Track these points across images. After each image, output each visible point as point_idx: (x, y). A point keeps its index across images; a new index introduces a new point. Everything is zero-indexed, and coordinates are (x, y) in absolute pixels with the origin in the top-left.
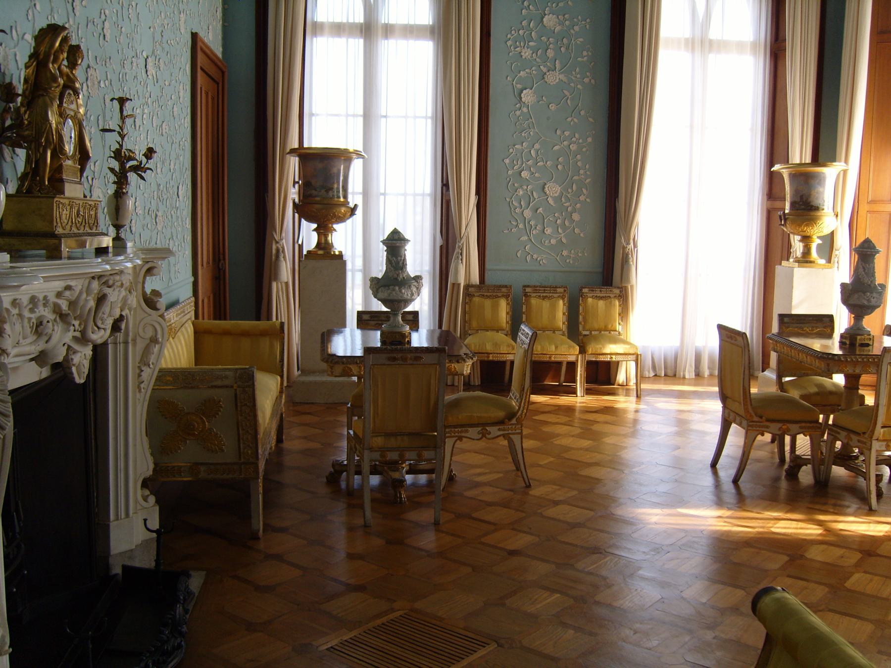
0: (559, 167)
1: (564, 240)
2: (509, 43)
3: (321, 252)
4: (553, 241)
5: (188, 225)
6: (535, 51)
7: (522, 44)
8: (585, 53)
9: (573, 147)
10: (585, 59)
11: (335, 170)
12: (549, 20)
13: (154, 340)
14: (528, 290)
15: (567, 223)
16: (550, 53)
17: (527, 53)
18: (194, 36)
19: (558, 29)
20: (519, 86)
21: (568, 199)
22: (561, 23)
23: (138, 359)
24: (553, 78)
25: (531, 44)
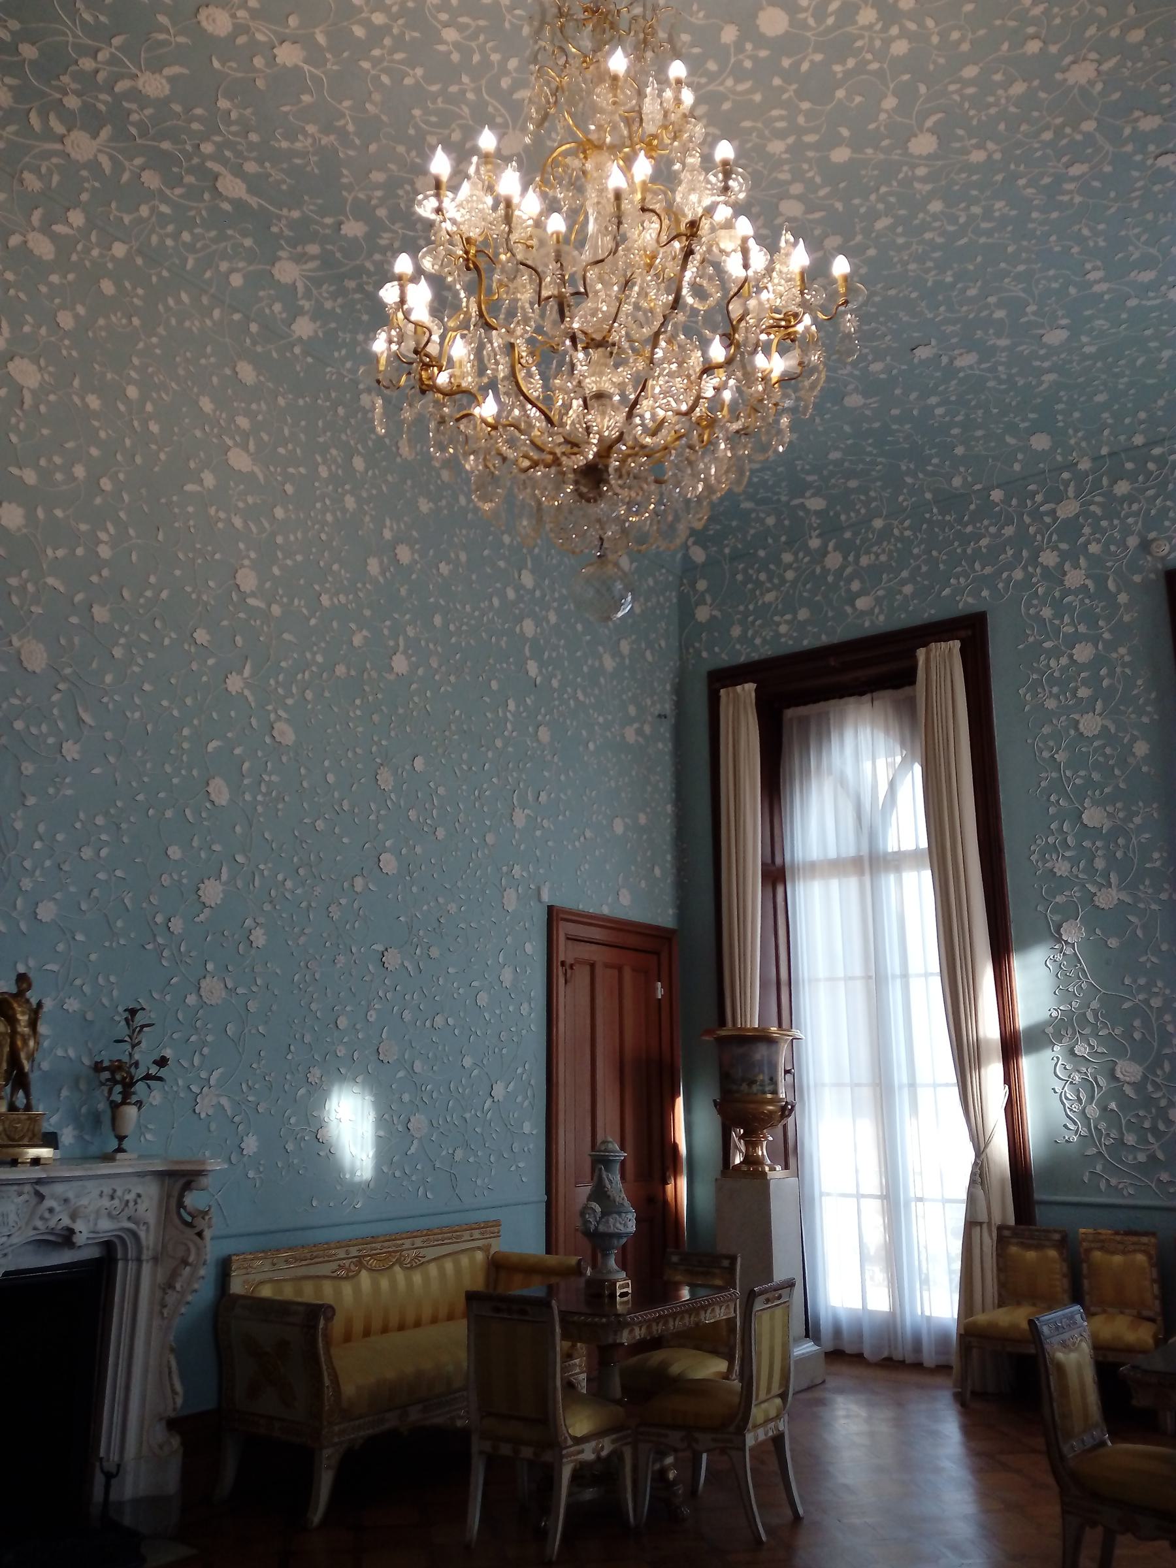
0: (1137, 1036)
1: (1160, 1156)
2: (1034, 858)
3: (745, 1168)
4: (1142, 1157)
5: (532, 1128)
6: (1074, 861)
7: (1054, 857)
8: (1156, 855)
9: (1156, 1002)
10: (1158, 864)
11: (758, 1057)
12: (1093, 816)
13: (185, 1262)
14: (1006, 1233)
15: (1162, 1127)
16: (1100, 864)
17: (1062, 868)
18: (550, 909)
19: (1107, 825)
20: (1057, 918)
21: (1157, 1086)
22: (1110, 816)
23: (160, 1278)
24: (1107, 898)
25: (1067, 854)
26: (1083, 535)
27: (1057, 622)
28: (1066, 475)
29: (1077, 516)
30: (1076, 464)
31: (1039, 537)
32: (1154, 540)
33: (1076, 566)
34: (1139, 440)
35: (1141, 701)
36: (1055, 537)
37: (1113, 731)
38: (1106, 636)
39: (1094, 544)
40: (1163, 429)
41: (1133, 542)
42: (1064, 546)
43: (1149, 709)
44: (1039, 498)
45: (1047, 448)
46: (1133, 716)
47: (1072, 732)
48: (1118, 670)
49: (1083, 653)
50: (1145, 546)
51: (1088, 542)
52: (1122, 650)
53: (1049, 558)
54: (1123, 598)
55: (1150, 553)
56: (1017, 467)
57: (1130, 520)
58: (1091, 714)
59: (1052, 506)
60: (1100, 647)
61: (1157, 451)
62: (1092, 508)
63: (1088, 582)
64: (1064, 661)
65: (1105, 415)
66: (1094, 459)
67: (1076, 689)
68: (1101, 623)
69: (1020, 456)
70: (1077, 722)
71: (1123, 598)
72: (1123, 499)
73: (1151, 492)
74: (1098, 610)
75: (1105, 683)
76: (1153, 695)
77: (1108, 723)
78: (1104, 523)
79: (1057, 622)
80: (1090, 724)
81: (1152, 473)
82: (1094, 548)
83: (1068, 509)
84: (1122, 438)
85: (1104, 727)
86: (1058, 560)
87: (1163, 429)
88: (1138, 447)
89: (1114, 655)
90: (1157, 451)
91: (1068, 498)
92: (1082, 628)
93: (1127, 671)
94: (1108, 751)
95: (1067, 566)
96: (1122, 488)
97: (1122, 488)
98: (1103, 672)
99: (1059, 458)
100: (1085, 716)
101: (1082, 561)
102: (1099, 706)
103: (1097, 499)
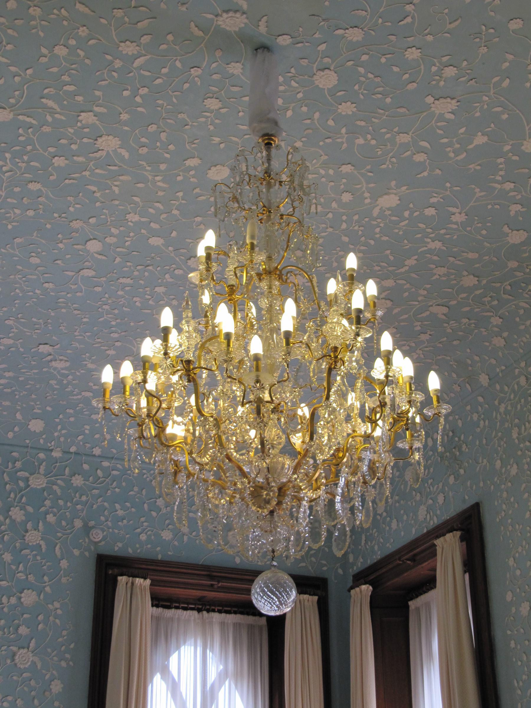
26: (45, 506)
27: (14, 567)
28: (42, 455)
29: (43, 490)
30: (52, 450)
31: (12, 495)
32: (93, 527)
33: (36, 529)
34: (97, 451)
35: (63, 648)
36: (24, 499)
37: (39, 667)
38: (48, 589)
39: (51, 515)
40: (114, 451)
41: (78, 523)
42: (30, 509)
43: (67, 656)
44: (18, 464)
45: (37, 431)
46: (55, 658)
47: (9, 661)
48: (51, 618)
49: (29, 598)
50: (87, 529)
51: (47, 513)
52: (57, 605)
53: (17, 514)
54: (64, 564)
55: (89, 537)
56: (10, 435)
57: (79, 507)
58: (25, 650)
59: (27, 474)
60: (42, 597)
61: (106, 464)
62: (55, 487)
63: (42, 543)
64: (13, 600)
65: (87, 427)
66: (65, 452)
67: (18, 626)
68: (46, 578)
69: (16, 429)
70: (14, 654)
71: (64, 564)
72: (77, 489)
73: (96, 492)
74: (45, 567)
75: (40, 627)
76: (72, 646)
77: (36, 659)
78: (61, 502)
79: (14, 567)
80: (25, 658)
81: (99, 478)
82: (50, 518)
83: (38, 482)
84: (88, 445)
85: (34, 663)
86: (24, 518)
87: (114, 451)
88: (94, 456)
89: (50, 606)
90: (106, 464)
91: (39, 473)
92: (31, 578)
93: (57, 621)
94: (33, 683)
95: (29, 526)
96: (77, 481)
97: (77, 481)
98: (41, 618)
99: (42, 441)
100: (21, 651)
101: (41, 524)
102: (32, 644)
103: (59, 482)
